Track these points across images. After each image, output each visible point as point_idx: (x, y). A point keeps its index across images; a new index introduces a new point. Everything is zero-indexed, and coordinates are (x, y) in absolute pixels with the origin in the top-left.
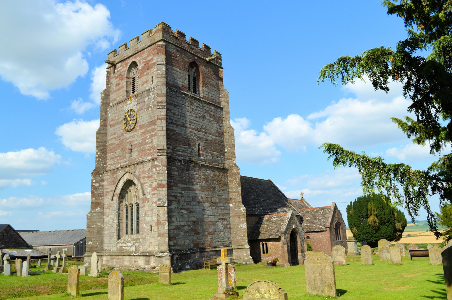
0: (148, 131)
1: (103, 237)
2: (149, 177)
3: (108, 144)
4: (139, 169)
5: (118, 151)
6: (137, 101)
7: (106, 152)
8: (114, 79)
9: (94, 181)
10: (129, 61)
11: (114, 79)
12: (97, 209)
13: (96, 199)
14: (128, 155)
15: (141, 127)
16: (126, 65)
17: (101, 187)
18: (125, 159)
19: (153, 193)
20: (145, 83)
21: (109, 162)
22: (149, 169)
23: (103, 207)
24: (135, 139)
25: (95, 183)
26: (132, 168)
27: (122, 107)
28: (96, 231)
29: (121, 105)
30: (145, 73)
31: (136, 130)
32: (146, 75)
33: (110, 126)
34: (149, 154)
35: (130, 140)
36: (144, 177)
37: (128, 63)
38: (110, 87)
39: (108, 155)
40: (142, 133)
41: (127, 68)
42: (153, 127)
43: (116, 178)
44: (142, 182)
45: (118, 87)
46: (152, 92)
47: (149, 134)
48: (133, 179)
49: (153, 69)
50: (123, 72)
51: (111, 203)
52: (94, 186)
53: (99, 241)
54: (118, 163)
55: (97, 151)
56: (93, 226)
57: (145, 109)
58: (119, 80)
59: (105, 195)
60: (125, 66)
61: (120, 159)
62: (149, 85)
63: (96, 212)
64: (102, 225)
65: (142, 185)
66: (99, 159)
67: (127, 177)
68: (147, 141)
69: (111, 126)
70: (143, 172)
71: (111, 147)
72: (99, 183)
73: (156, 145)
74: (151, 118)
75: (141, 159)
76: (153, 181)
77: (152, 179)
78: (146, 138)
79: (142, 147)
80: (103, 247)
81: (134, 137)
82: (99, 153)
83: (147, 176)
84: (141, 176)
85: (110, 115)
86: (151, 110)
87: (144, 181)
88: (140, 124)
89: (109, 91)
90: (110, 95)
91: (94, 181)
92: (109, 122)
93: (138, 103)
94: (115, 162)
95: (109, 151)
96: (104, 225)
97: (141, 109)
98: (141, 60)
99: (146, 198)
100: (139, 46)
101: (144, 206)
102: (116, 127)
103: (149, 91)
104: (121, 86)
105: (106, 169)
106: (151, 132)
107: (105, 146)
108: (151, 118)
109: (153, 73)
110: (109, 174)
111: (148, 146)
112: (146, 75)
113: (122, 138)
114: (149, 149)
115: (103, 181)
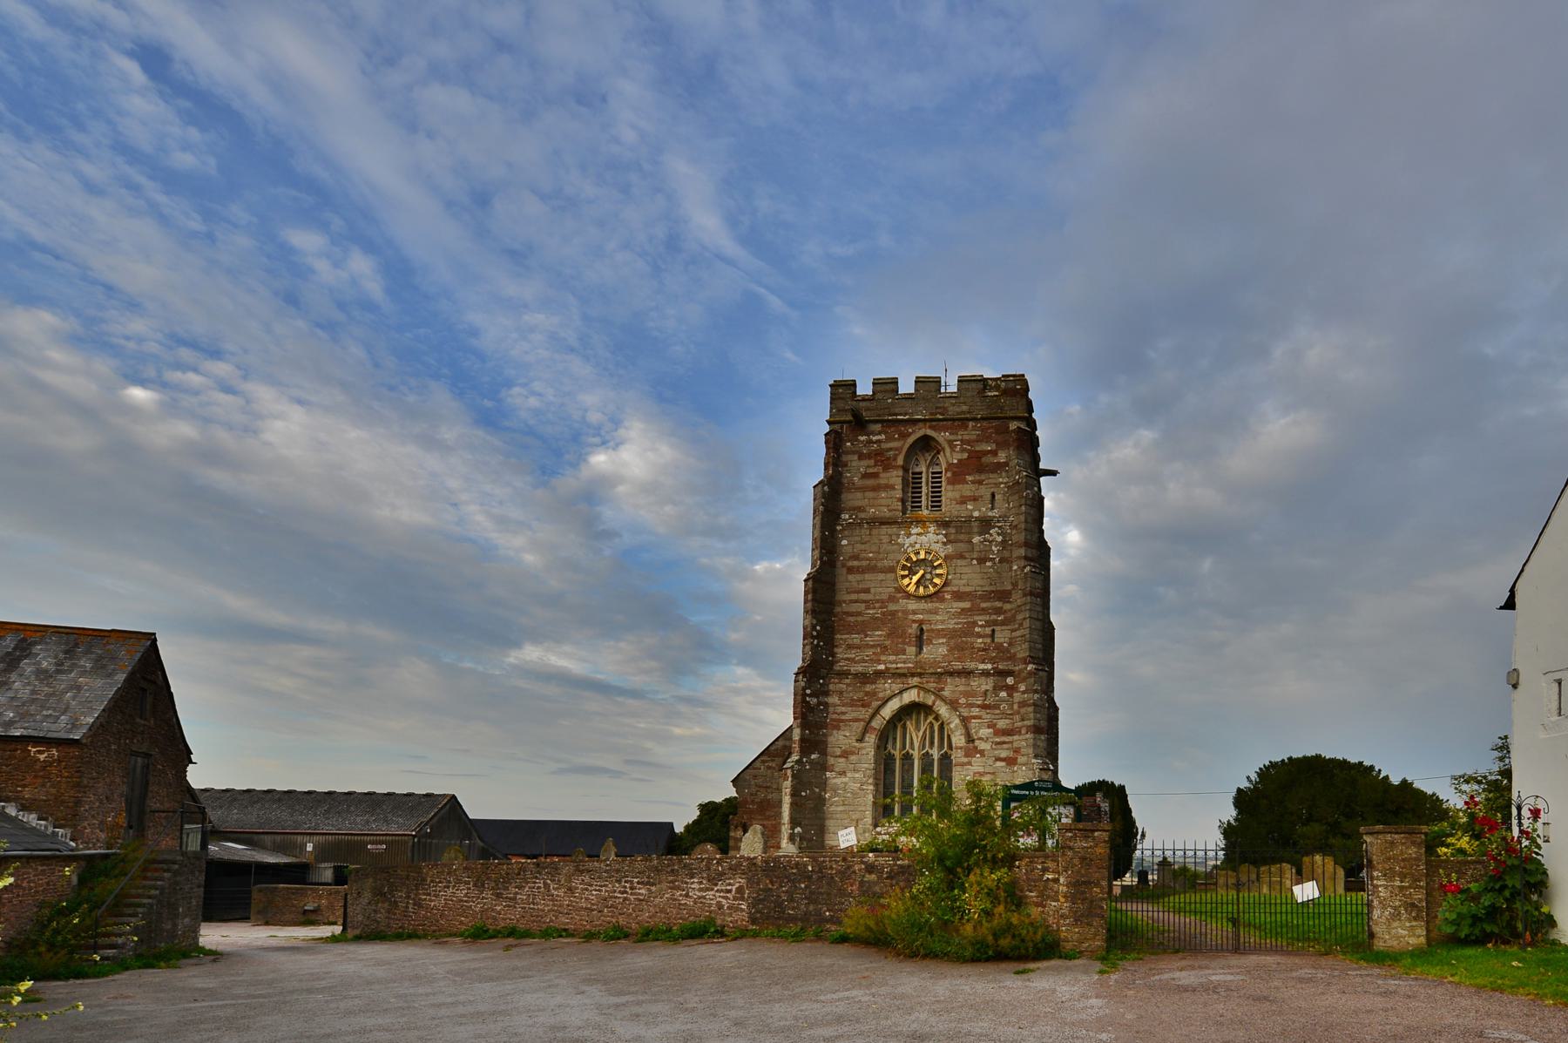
0: (983, 609)
1: (824, 819)
2: (984, 707)
3: (838, 609)
4: (951, 688)
5: (880, 633)
6: (945, 536)
7: (833, 627)
8: (856, 457)
9: (808, 692)
10: (914, 431)
11: (856, 457)
12: (813, 756)
13: (811, 733)
14: (912, 650)
15: (958, 596)
16: (904, 436)
17: (822, 707)
18: (905, 657)
19: (998, 740)
20: (970, 501)
21: (840, 652)
22: (987, 690)
23: (824, 753)
24: (938, 618)
25: (809, 695)
26: (932, 680)
27: (891, 535)
28: (810, 804)
29: (894, 529)
30: (969, 478)
31: (943, 600)
32: (973, 482)
33: (844, 571)
34: (985, 659)
35: (921, 617)
36: (970, 704)
37: (911, 434)
38: (841, 474)
39: (836, 637)
40: (963, 610)
41: (907, 446)
42: (998, 604)
43: (874, 694)
44: (966, 714)
45: (870, 482)
46: (996, 529)
47: (987, 618)
48: (934, 704)
49: (995, 475)
50: (891, 449)
51: (855, 747)
52: (809, 702)
53: (815, 827)
54: (879, 662)
55: (815, 622)
56: (803, 794)
57: (972, 559)
58: (875, 466)
59: (829, 726)
60: (896, 436)
61: (883, 653)
62: (984, 509)
63: (811, 762)
64: (823, 793)
65: (965, 721)
66: (818, 643)
67: (911, 696)
68: (977, 629)
69: (850, 570)
70: (967, 694)
71: (852, 619)
72: (818, 697)
73: (1005, 645)
74: (991, 584)
75: (958, 665)
76: (997, 717)
77: (998, 712)
78: (975, 624)
79: (962, 641)
80: (823, 841)
81: (936, 613)
82: (818, 628)
83: (979, 702)
84: (963, 701)
85: (844, 542)
86: (991, 567)
87: (970, 712)
88: (955, 589)
89: (840, 483)
90: (842, 492)
91: (808, 692)
92: (842, 558)
93: (949, 542)
94: (867, 656)
95: (841, 628)
96: (826, 793)
97: (961, 556)
98: (955, 441)
99: (976, 748)
100: (946, 405)
101: (970, 763)
102: (867, 576)
103: (986, 524)
104: (882, 482)
105: (831, 669)
106: (990, 614)
107: (831, 613)
108: (991, 584)
109: (995, 484)
110: (848, 681)
111: (980, 640)
112: (973, 482)
113: (892, 607)
114: (984, 650)
115: (827, 694)
